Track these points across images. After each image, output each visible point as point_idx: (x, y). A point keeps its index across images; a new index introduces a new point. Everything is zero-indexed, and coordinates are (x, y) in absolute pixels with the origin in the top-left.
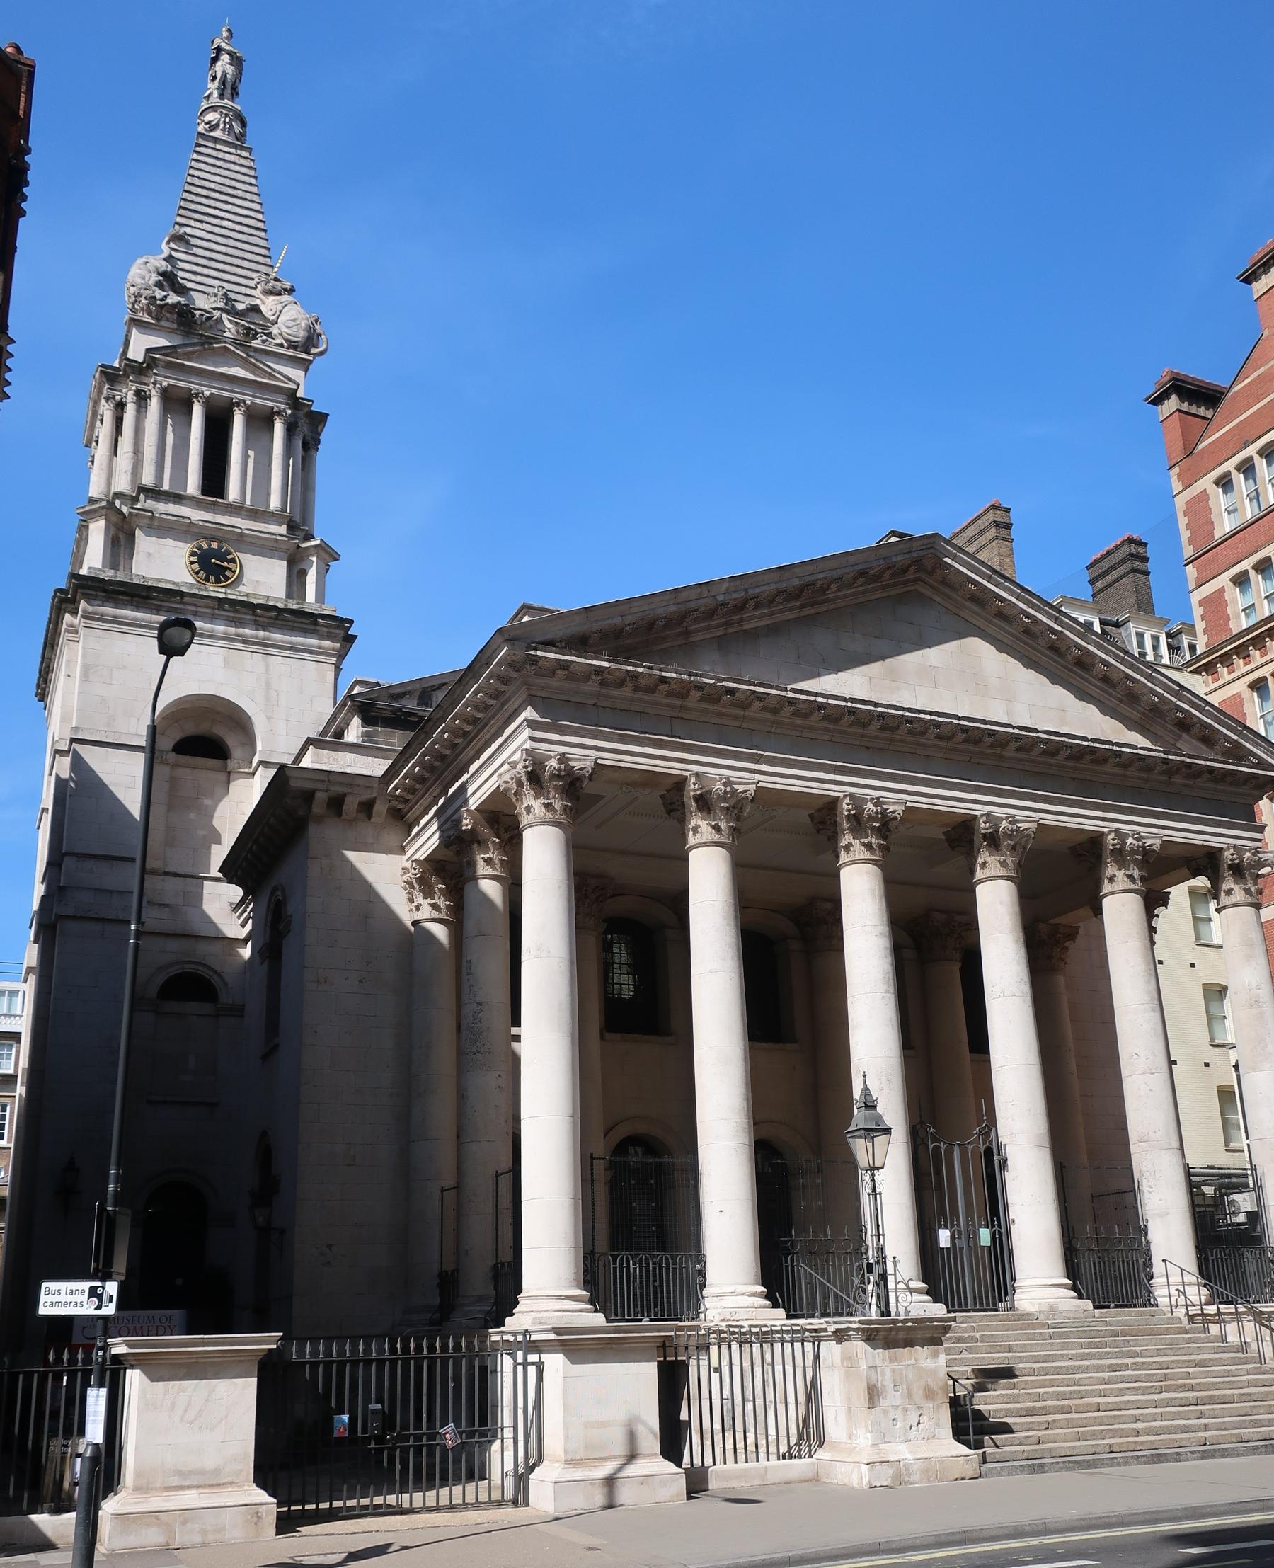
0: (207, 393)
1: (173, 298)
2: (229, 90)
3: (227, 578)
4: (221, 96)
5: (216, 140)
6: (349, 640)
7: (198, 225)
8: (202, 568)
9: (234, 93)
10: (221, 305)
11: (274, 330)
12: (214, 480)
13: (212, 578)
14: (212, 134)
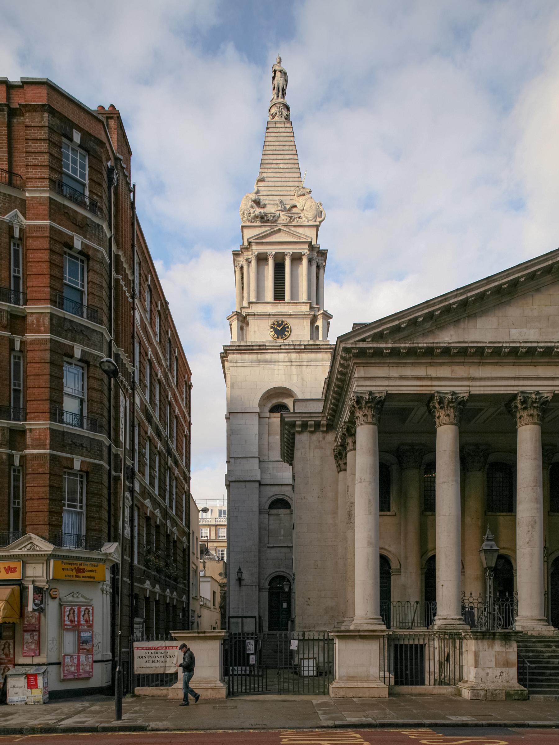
0: (274, 253)
1: (258, 211)
2: (280, 93)
3: (285, 335)
4: (278, 96)
5: (276, 122)
7: (269, 170)
8: (275, 333)
9: (284, 94)
10: (279, 208)
12: (279, 295)
13: (280, 337)
14: (274, 120)
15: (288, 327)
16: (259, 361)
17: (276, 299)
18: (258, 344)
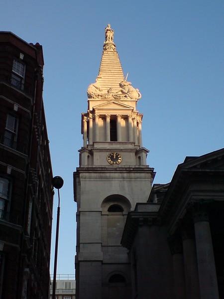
6: (153, 174)
11: (127, 95)
15: (120, 157)
16: (101, 178)
17: (111, 140)
18: (101, 167)
